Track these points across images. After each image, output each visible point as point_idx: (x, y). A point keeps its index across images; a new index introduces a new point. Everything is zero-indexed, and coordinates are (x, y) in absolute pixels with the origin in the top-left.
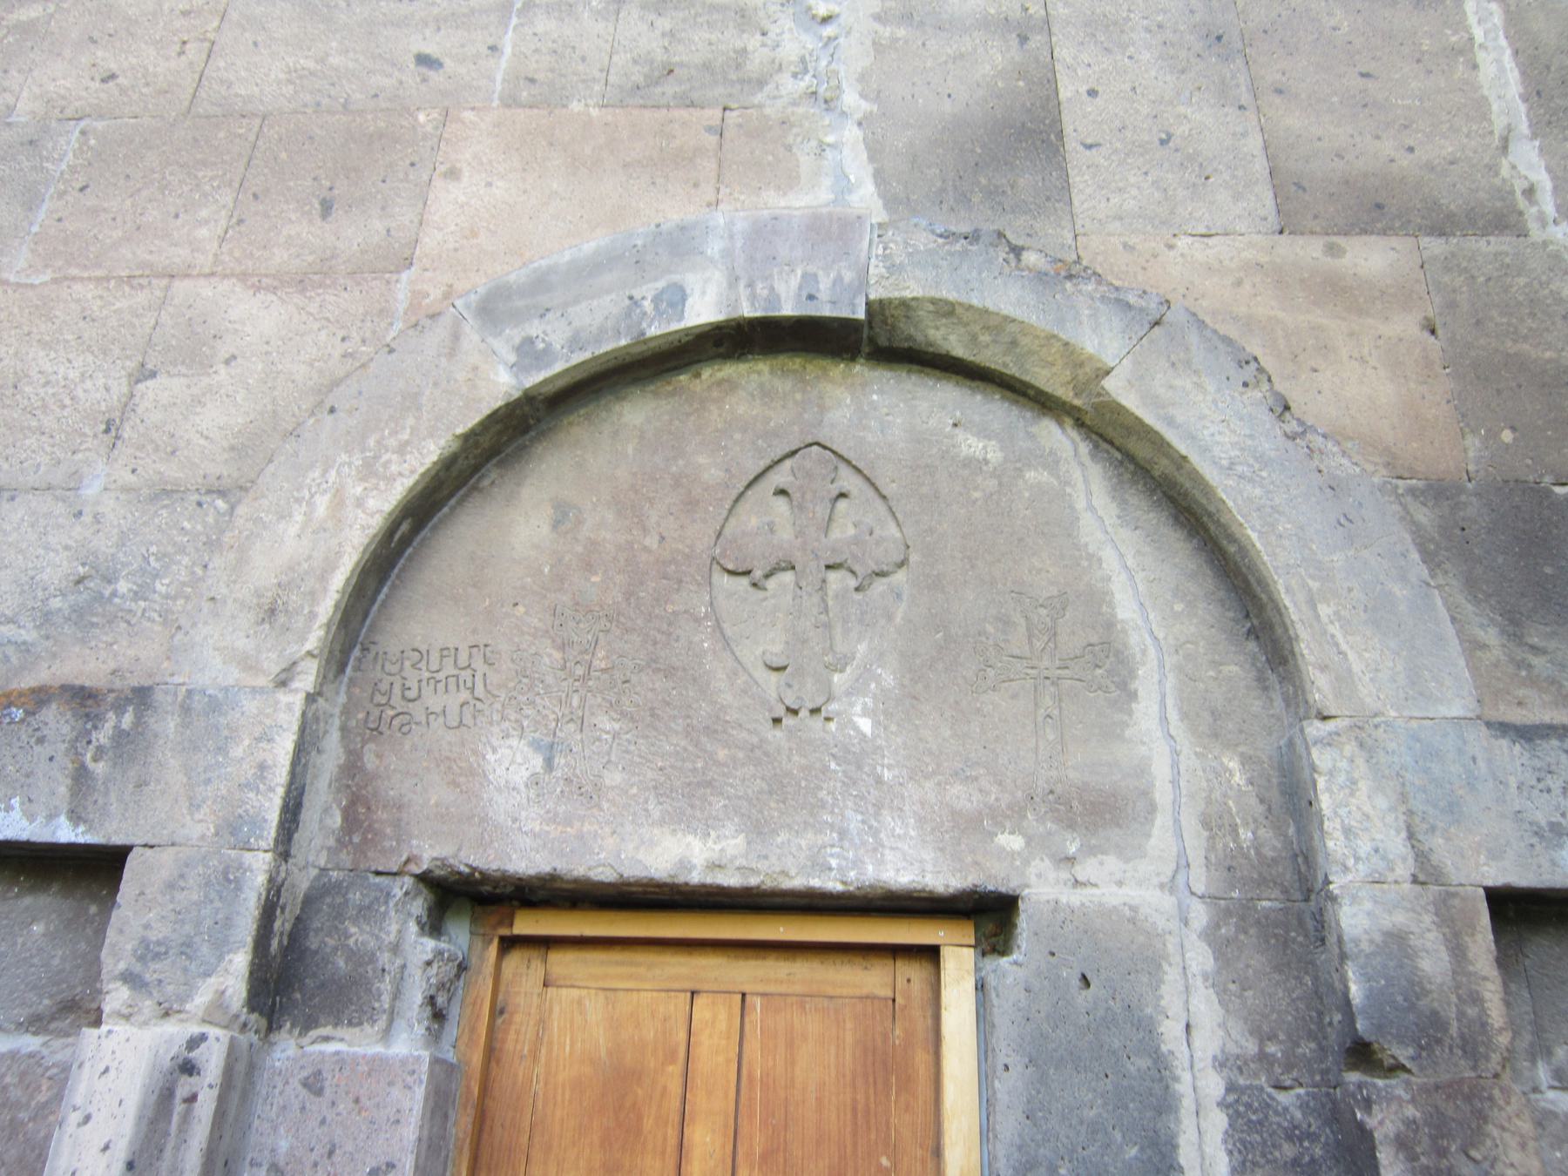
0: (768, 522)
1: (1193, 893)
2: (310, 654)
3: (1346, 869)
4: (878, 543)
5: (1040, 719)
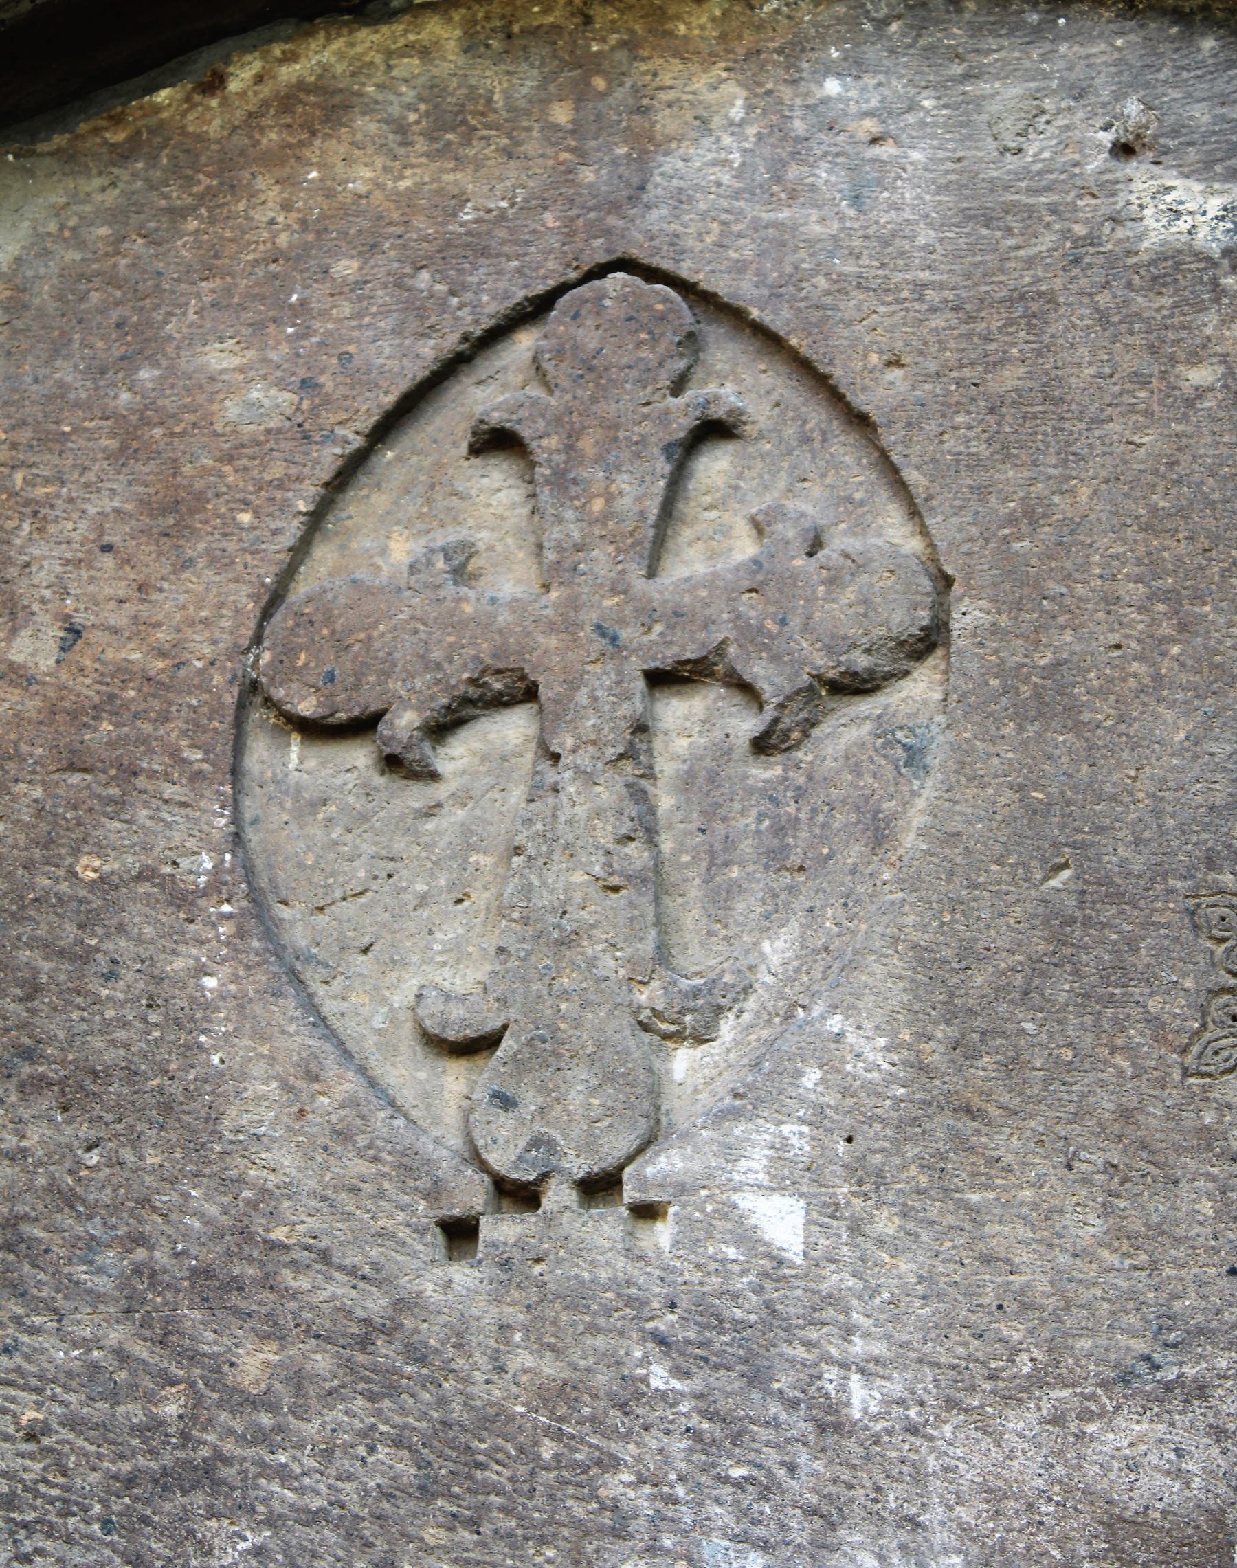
0: (454, 542)
4: (833, 582)
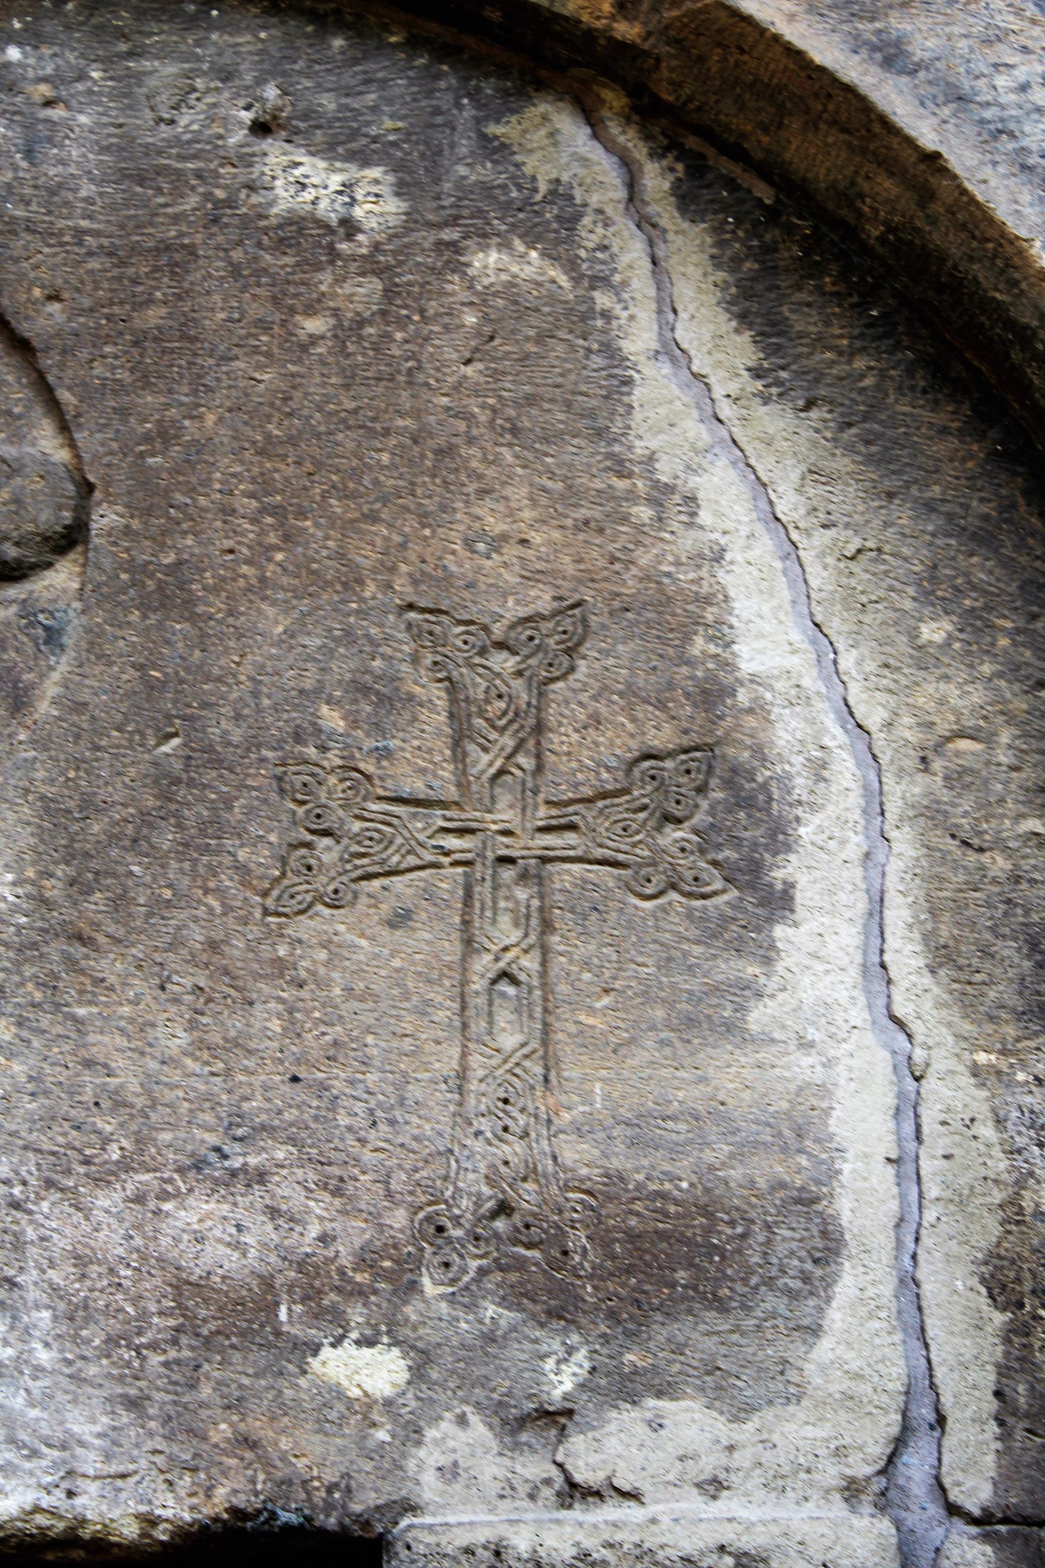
1: (953, 1510)
5: (478, 985)
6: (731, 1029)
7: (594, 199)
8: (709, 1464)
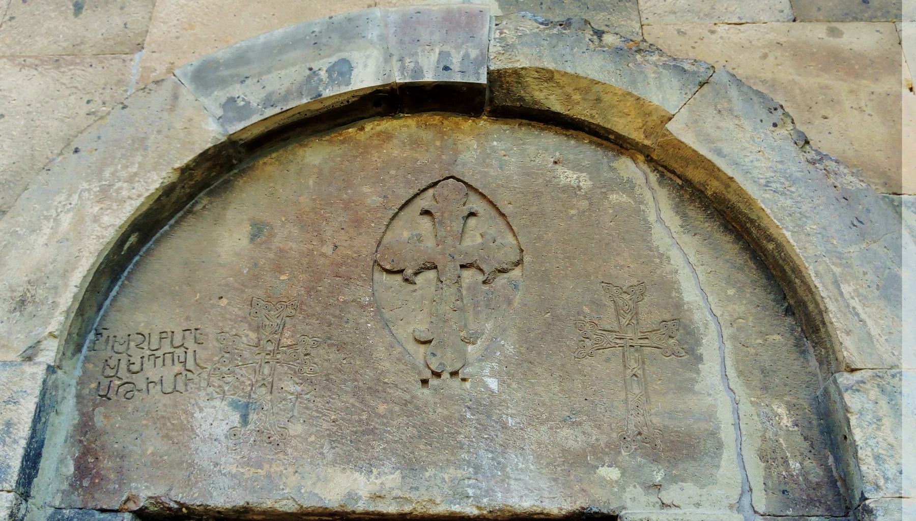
1: (756, 512)
2: (51, 334)
3: (878, 487)
6: (691, 390)
7: (638, 182)
8: (696, 499)
